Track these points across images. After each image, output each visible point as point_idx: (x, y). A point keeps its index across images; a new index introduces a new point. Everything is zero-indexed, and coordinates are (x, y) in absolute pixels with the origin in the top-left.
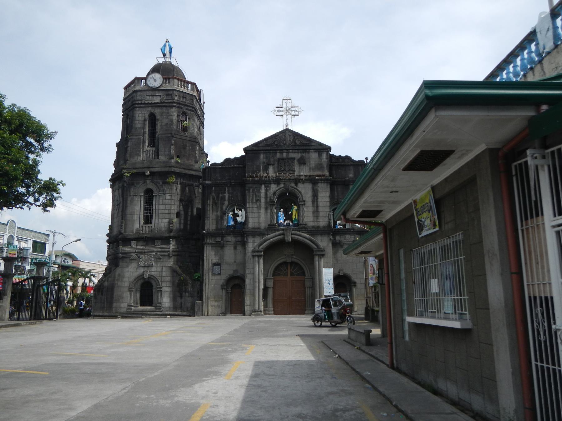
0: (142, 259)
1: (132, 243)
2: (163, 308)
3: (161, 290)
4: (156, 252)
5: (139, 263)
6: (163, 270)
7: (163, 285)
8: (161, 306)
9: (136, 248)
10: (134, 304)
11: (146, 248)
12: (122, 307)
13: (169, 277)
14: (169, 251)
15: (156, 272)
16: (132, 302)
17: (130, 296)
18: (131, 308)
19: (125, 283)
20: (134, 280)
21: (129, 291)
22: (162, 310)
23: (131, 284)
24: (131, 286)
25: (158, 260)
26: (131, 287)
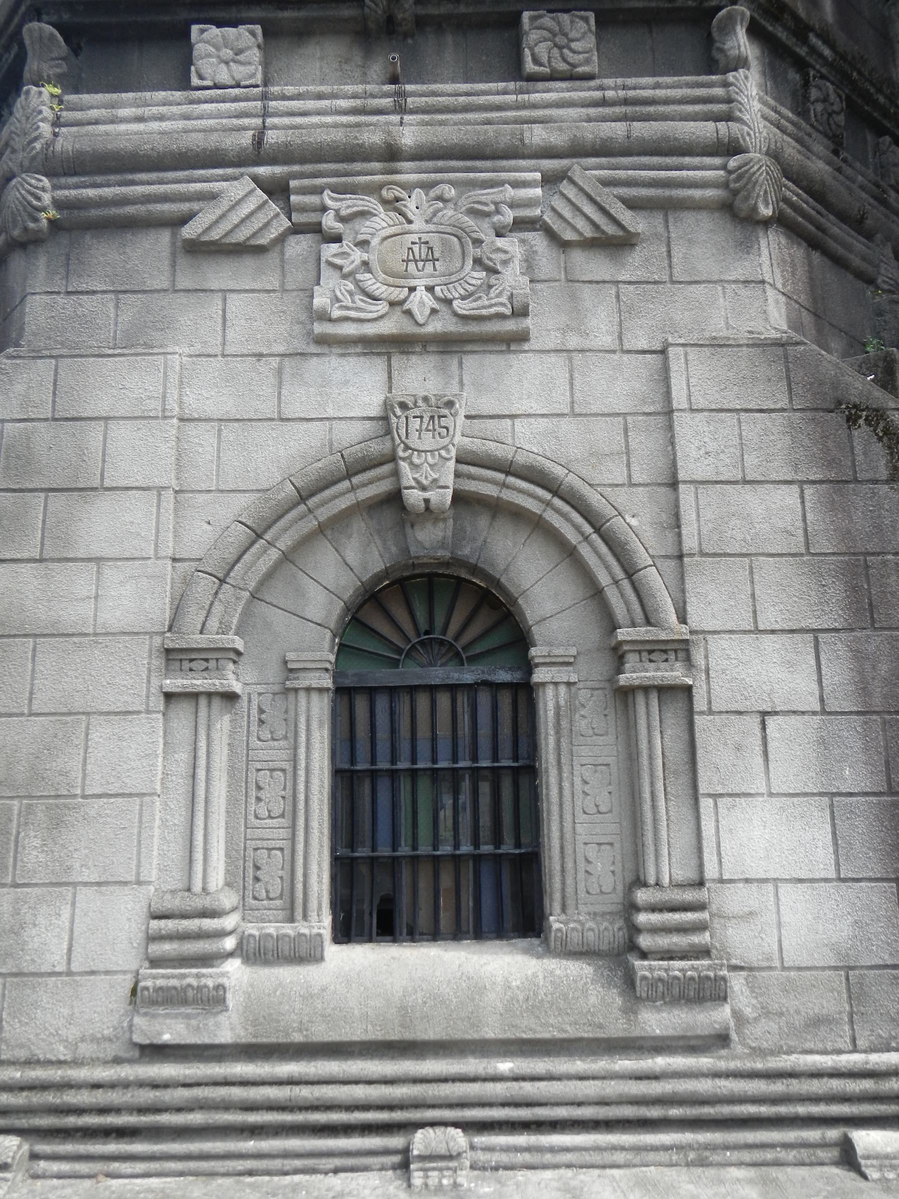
0: (363, 244)
1: (200, 49)
2: (737, 983)
3: (688, 690)
4: (548, 153)
5: (320, 301)
6: (679, 398)
7: (698, 616)
8: (704, 952)
9: (265, 114)
10: (243, 907)
11: (401, 109)
12: (55, 959)
13: (789, 497)
14: (732, 148)
15: (566, 426)
16: (217, 877)
17: (179, 784)
18: (209, 977)
19: (110, 573)
20: (240, 533)
21: (169, 696)
22: (722, 1015)
23: (205, 586)
24: (193, 617)
25: (578, 257)
26: (198, 640)
